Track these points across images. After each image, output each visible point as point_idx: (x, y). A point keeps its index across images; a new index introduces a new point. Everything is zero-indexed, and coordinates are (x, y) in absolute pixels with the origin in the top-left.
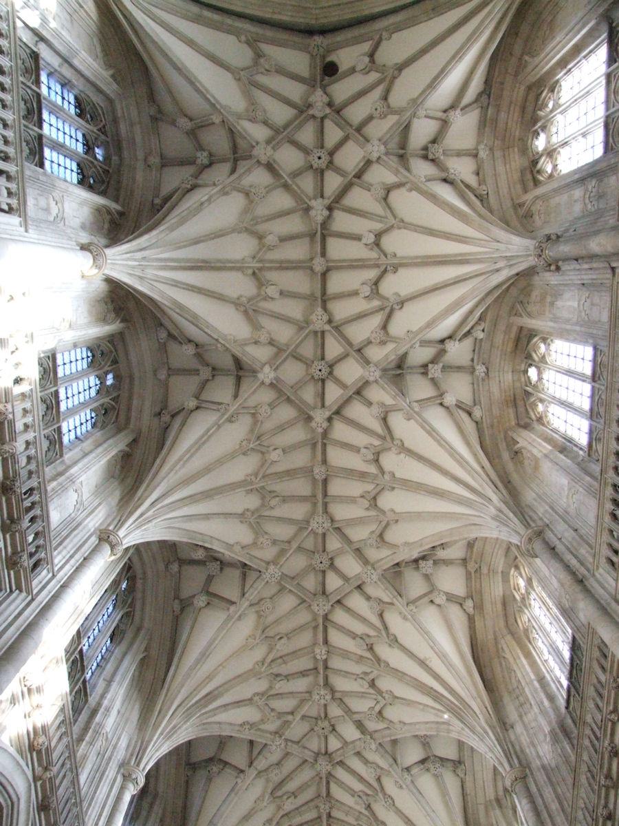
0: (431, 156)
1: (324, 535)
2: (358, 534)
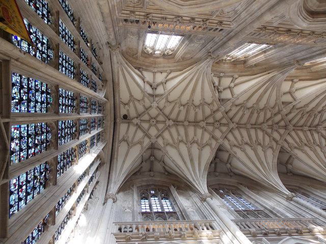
2: (269, 115)
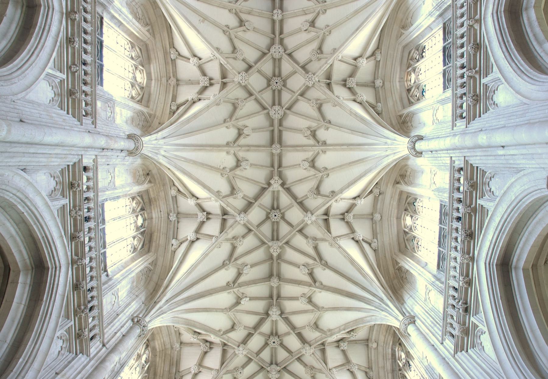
0: (208, 344)
1: (274, 104)
